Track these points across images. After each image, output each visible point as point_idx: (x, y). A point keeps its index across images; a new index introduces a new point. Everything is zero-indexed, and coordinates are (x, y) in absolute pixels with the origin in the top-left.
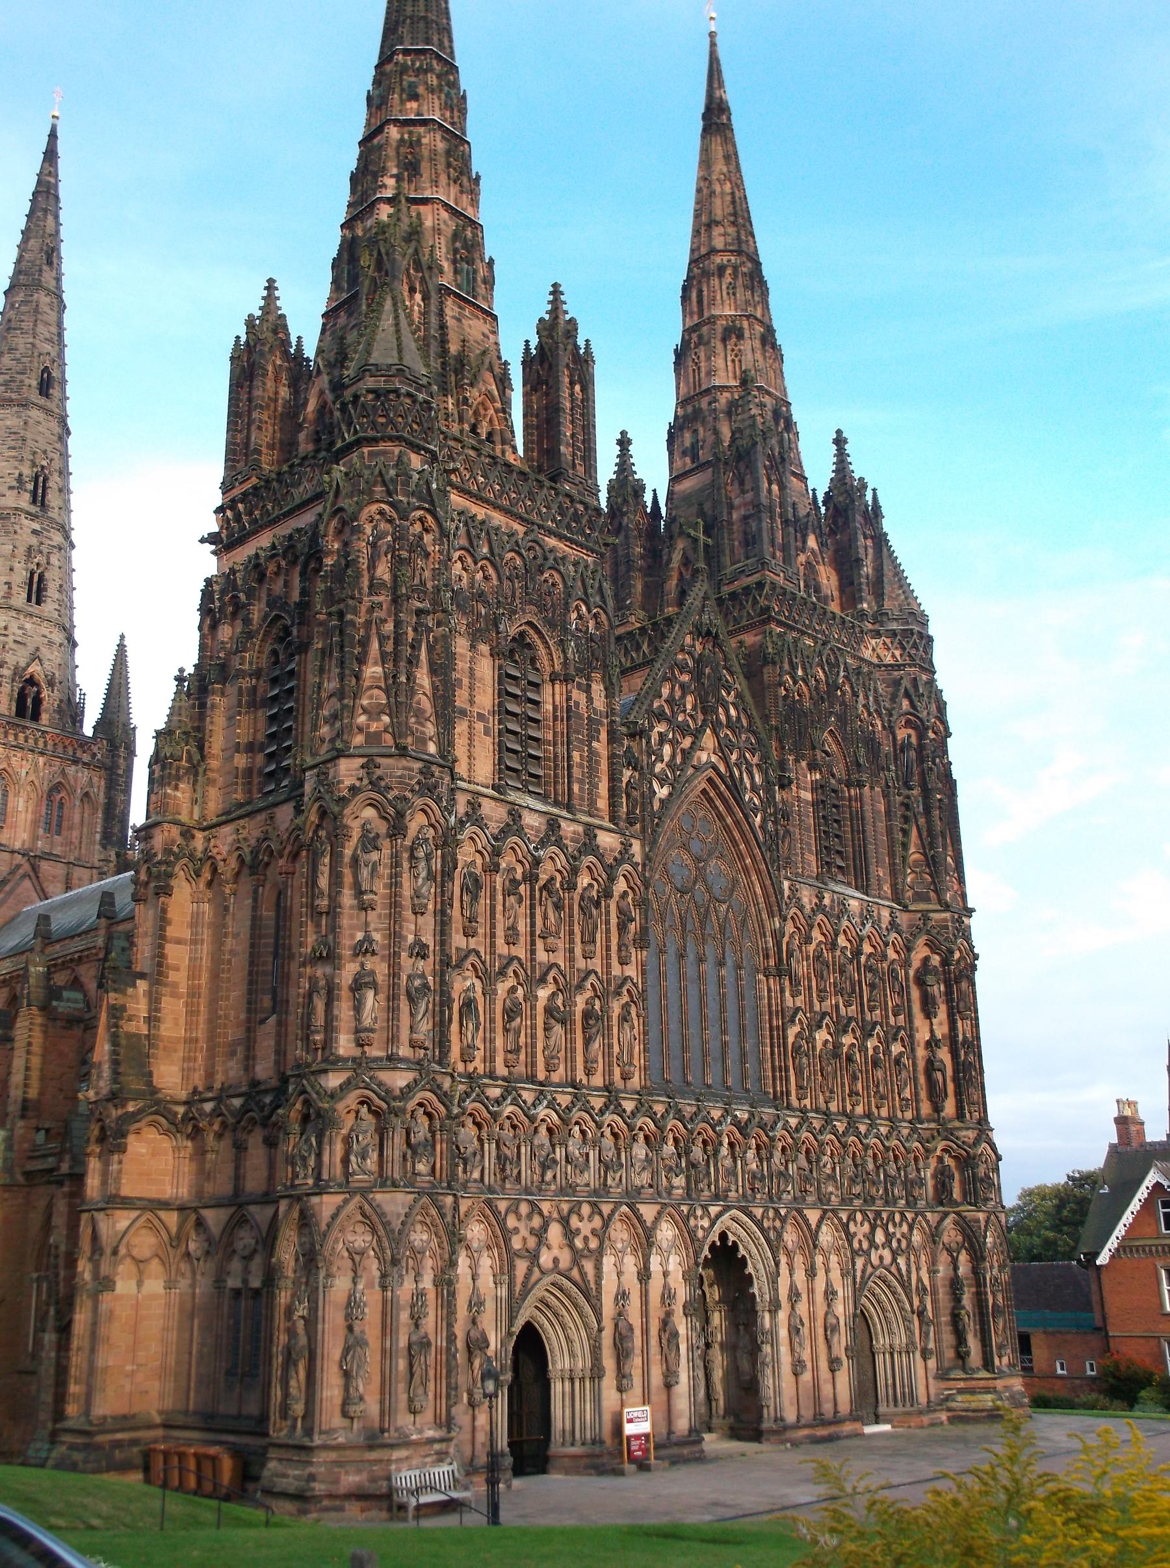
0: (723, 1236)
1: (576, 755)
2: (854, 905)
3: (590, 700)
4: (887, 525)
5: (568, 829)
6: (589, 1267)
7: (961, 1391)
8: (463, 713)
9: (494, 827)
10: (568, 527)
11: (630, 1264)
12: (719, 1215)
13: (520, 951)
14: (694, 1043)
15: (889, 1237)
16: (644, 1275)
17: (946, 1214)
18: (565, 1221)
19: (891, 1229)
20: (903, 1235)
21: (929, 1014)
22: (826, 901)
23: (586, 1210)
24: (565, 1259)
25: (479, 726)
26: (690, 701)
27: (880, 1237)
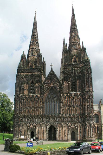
0: (52, 125)
1: (37, 90)
2: (73, 94)
3: (38, 84)
4: (86, 50)
5: (34, 96)
6: (35, 127)
7: (84, 139)
8: (25, 90)
9: (27, 97)
10: (37, 71)
11: (40, 127)
12: (49, 124)
13: (30, 106)
14: (48, 110)
15: (74, 125)
16: (41, 128)
17: (84, 122)
18: (32, 124)
19: (75, 124)
20: (77, 125)
21: (84, 103)
22: (68, 94)
23: (35, 124)
24: (32, 127)
25: (27, 90)
26: (49, 81)
27: (73, 125)
